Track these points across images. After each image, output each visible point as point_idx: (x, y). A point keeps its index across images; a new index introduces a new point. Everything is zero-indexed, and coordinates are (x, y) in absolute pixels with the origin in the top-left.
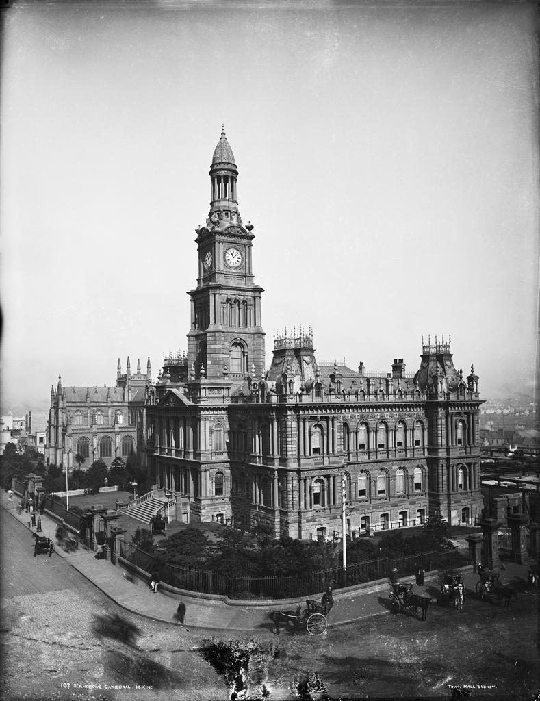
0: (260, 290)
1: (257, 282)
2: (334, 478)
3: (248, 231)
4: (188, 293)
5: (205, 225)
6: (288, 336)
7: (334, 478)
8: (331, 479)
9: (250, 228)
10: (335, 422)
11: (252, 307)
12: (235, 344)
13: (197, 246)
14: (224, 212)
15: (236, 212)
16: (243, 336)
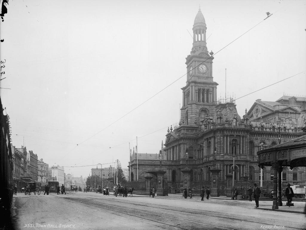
0: (217, 84)
1: (215, 80)
2: (243, 166)
3: (210, 56)
4: (182, 89)
5: (190, 54)
6: (222, 98)
7: (243, 166)
8: (242, 167)
9: (212, 53)
10: (244, 139)
11: (212, 93)
12: (202, 111)
13: (186, 66)
14: (199, 47)
15: (205, 47)
16: (206, 107)
